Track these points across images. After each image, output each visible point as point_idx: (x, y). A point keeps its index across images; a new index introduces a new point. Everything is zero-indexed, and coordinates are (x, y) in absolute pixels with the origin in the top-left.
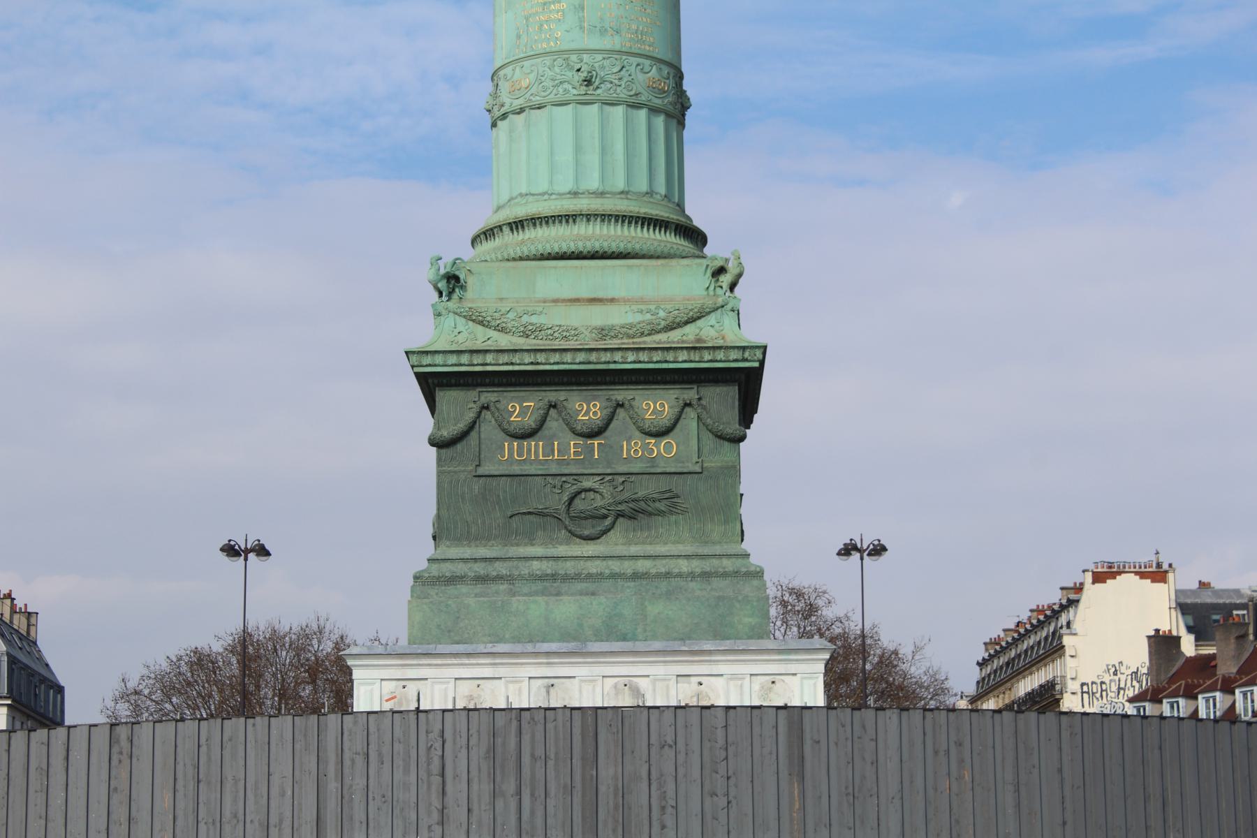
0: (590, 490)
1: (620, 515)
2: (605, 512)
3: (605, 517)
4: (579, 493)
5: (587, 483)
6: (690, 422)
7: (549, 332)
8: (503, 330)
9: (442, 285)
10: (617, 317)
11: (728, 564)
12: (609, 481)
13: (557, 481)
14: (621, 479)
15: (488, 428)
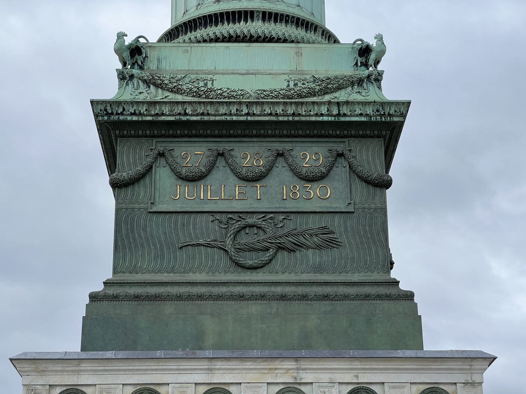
0: (251, 226)
1: (281, 248)
2: (268, 245)
3: (267, 249)
4: (244, 228)
5: (250, 220)
6: (341, 171)
7: (219, 92)
8: (177, 90)
9: (126, 54)
10: (279, 84)
11: (383, 290)
12: (271, 218)
13: (224, 218)
14: (281, 217)
15: (163, 175)
